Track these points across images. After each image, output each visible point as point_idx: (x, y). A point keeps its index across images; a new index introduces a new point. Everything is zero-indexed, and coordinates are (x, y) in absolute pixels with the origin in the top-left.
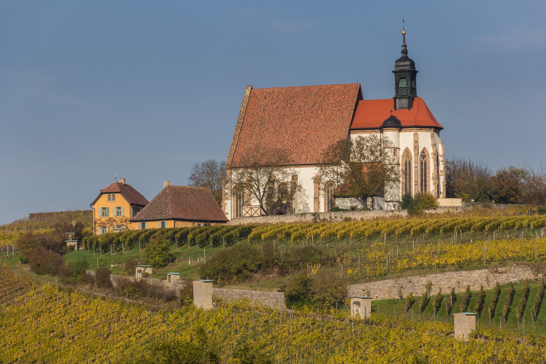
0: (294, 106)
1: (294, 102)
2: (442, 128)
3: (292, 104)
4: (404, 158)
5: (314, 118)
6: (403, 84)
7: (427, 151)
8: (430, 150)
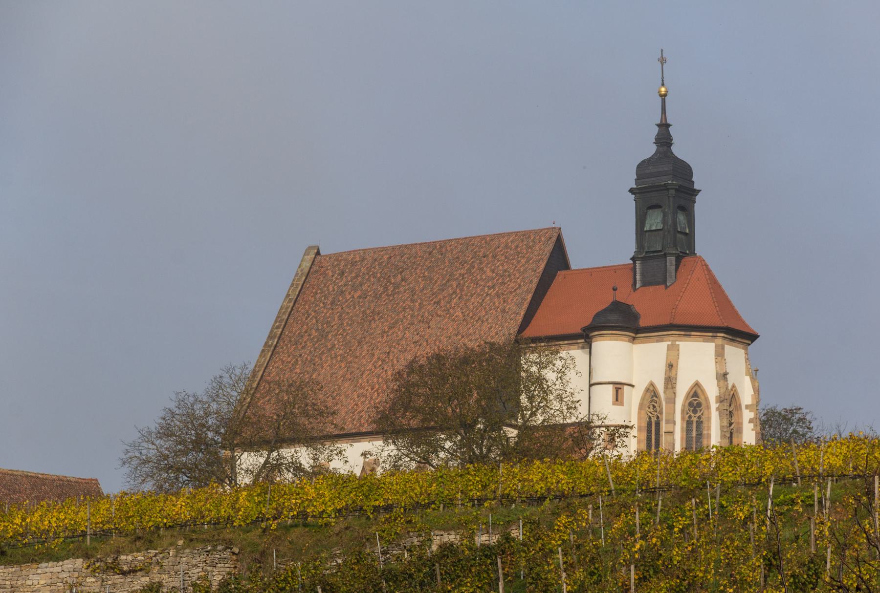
0: (402, 289)
1: (402, 280)
3: (397, 286)
4: (643, 412)
5: (440, 316)
6: (655, 221)
7: (703, 391)
8: (712, 391)
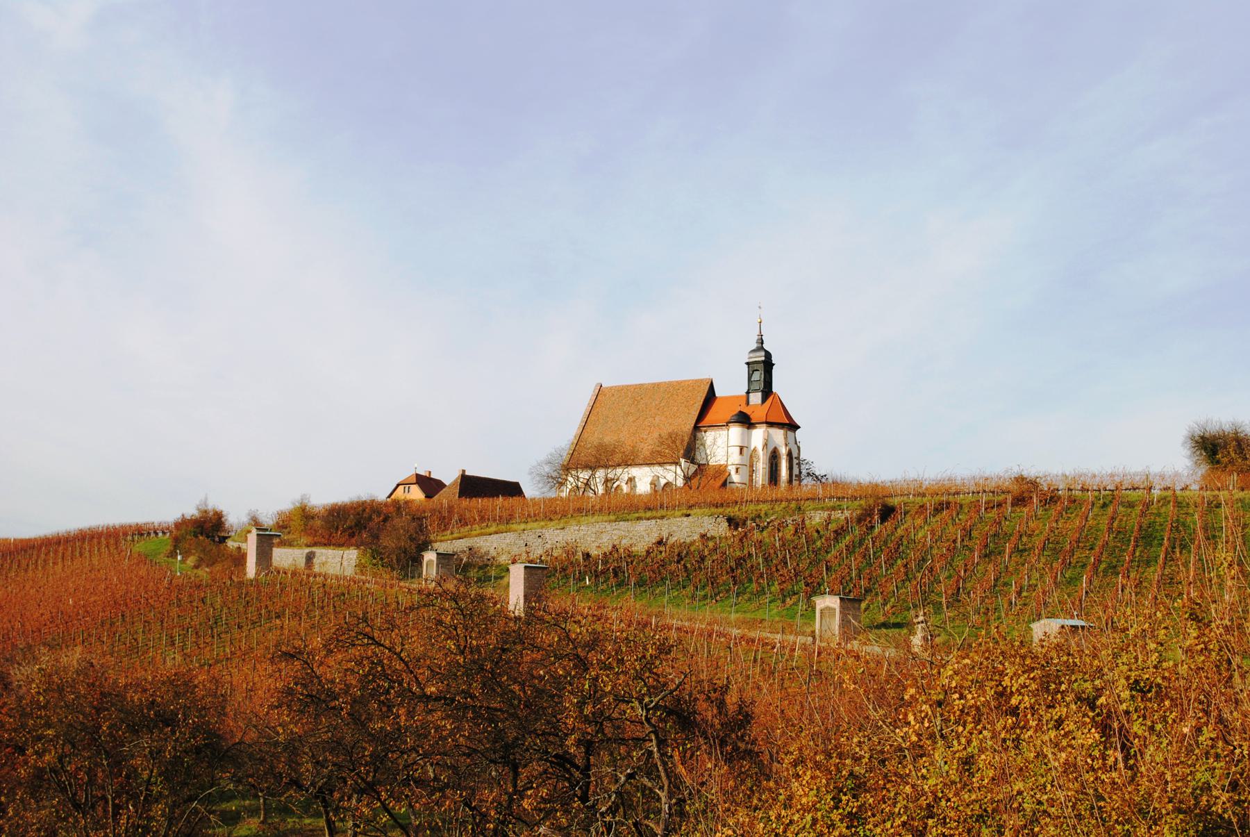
2: (799, 427)
6: (756, 376)
